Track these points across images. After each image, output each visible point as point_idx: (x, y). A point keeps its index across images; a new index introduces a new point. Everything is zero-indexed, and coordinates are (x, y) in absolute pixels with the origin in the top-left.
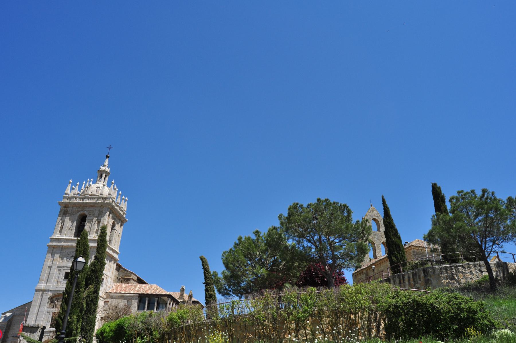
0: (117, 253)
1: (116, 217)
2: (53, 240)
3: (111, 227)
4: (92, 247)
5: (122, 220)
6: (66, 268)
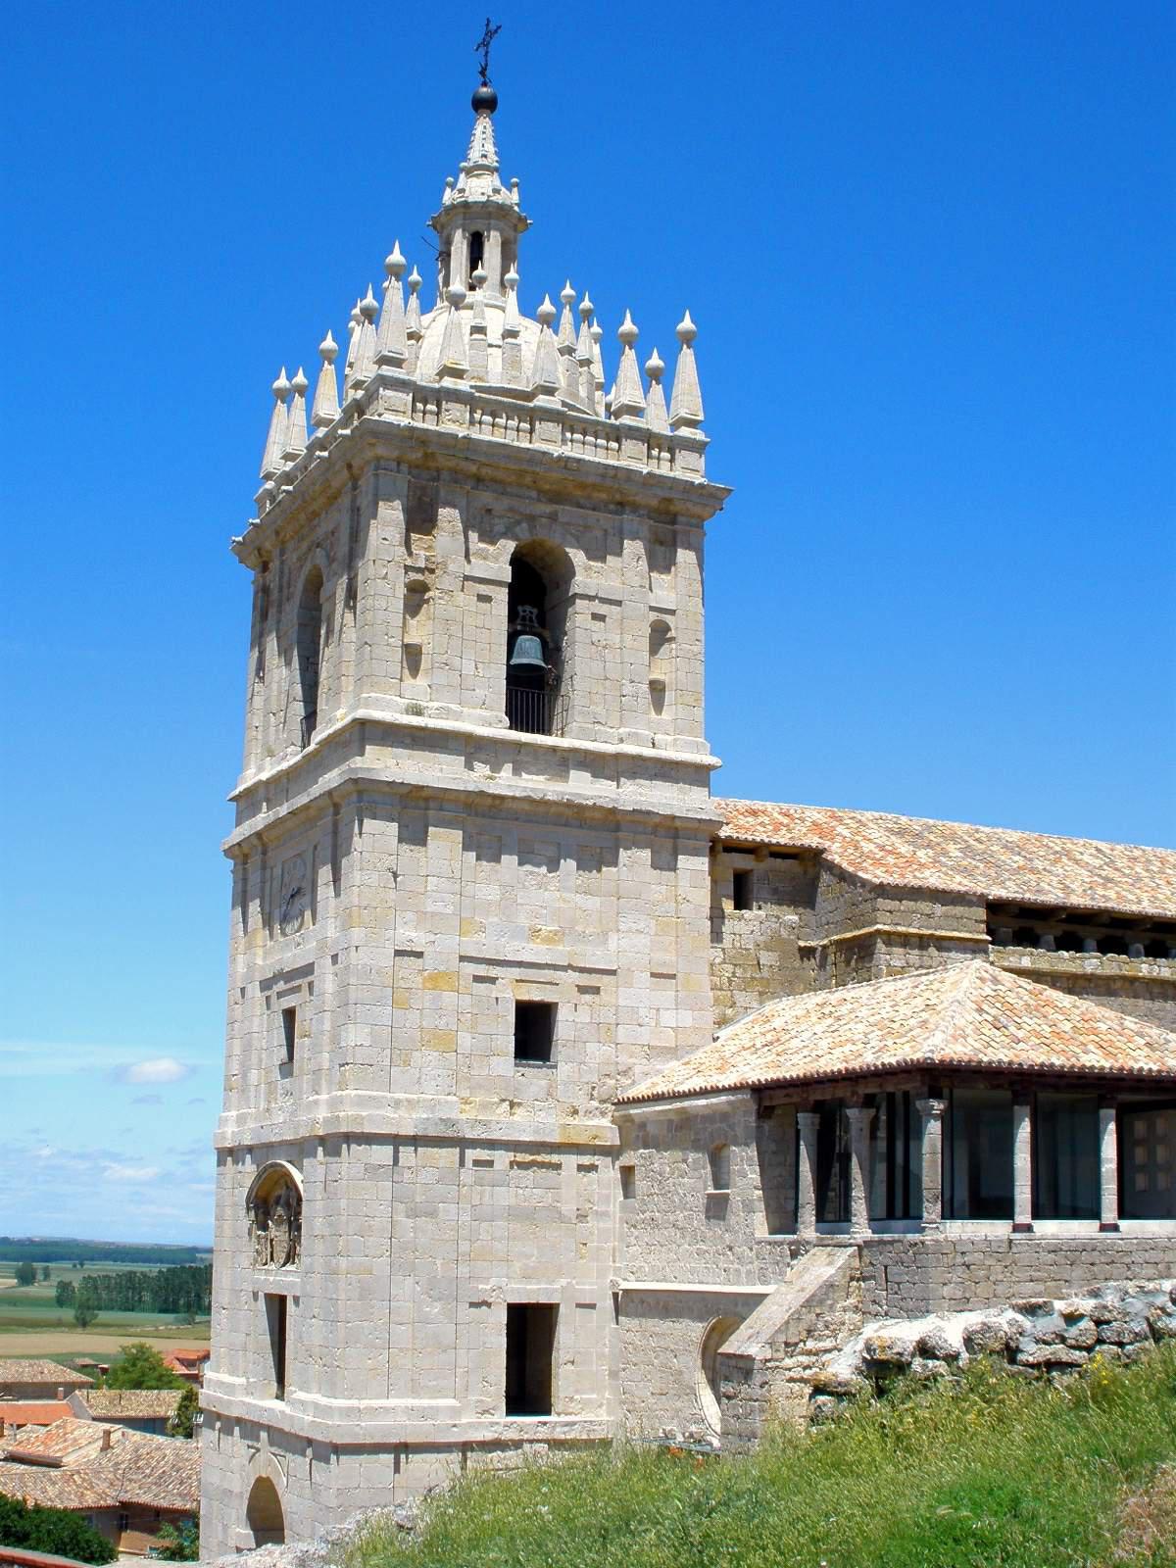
0: (696, 775)
1: (557, 497)
2: (248, 802)
3: (502, 596)
4: (337, 799)
5: (654, 503)
6: (281, 986)
